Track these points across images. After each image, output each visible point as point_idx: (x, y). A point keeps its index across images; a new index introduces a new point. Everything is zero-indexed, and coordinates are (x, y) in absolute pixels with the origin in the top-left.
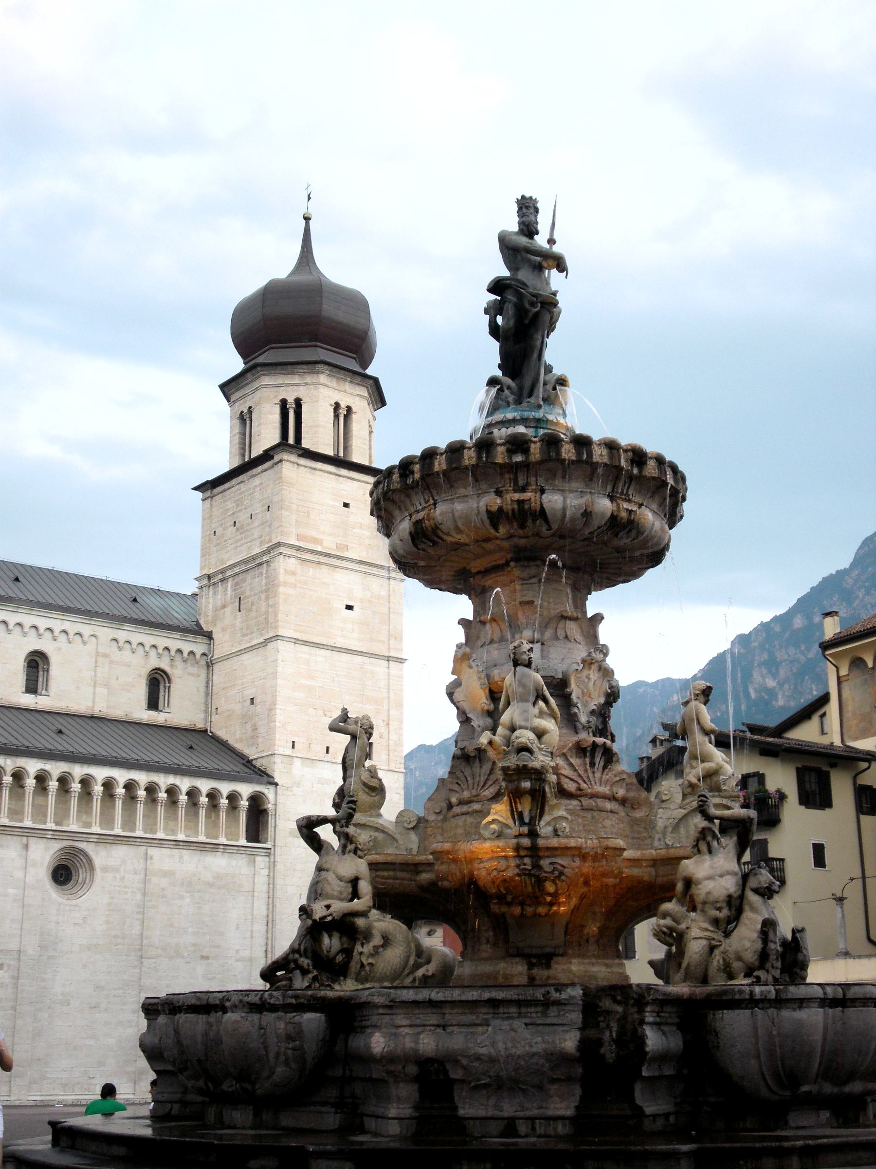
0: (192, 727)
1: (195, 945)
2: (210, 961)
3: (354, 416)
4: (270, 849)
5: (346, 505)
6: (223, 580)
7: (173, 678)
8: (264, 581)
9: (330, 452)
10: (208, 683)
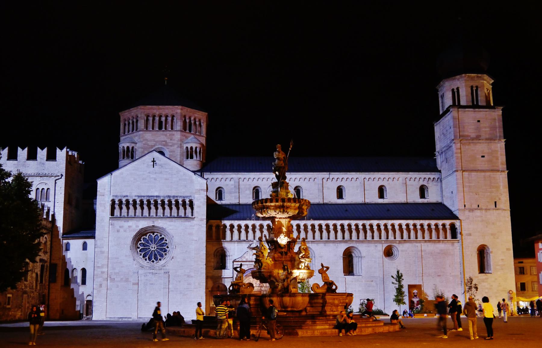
0: (437, 202)
1: (435, 272)
2: (441, 277)
3: (479, 89)
4: (459, 240)
5: (479, 121)
6: (442, 153)
7: (428, 187)
8: (451, 153)
9: (471, 104)
10: (441, 187)
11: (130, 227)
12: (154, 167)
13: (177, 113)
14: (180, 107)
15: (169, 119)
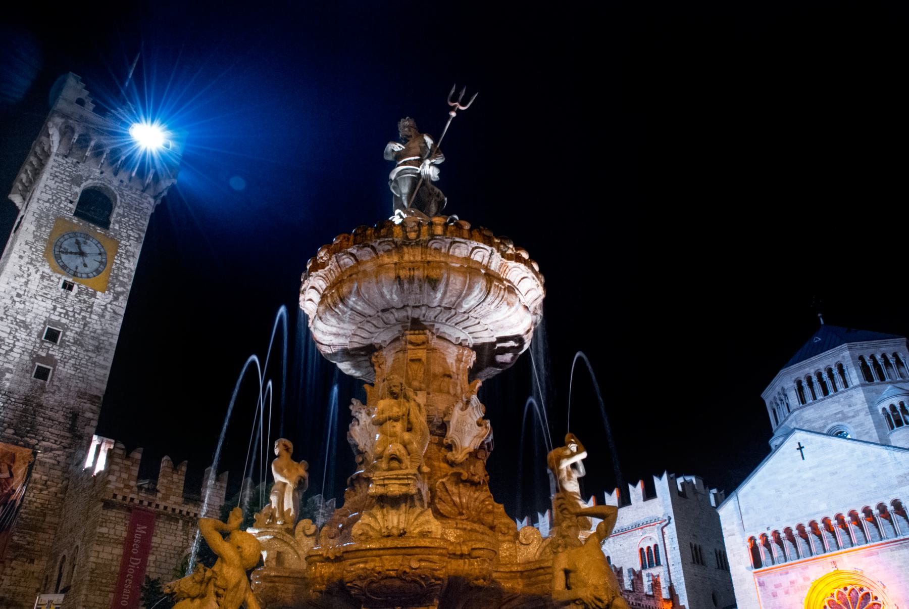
11: (792, 582)
12: (803, 459)
13: (843, 357)
14: (845, 345)
15: (835, 371)
